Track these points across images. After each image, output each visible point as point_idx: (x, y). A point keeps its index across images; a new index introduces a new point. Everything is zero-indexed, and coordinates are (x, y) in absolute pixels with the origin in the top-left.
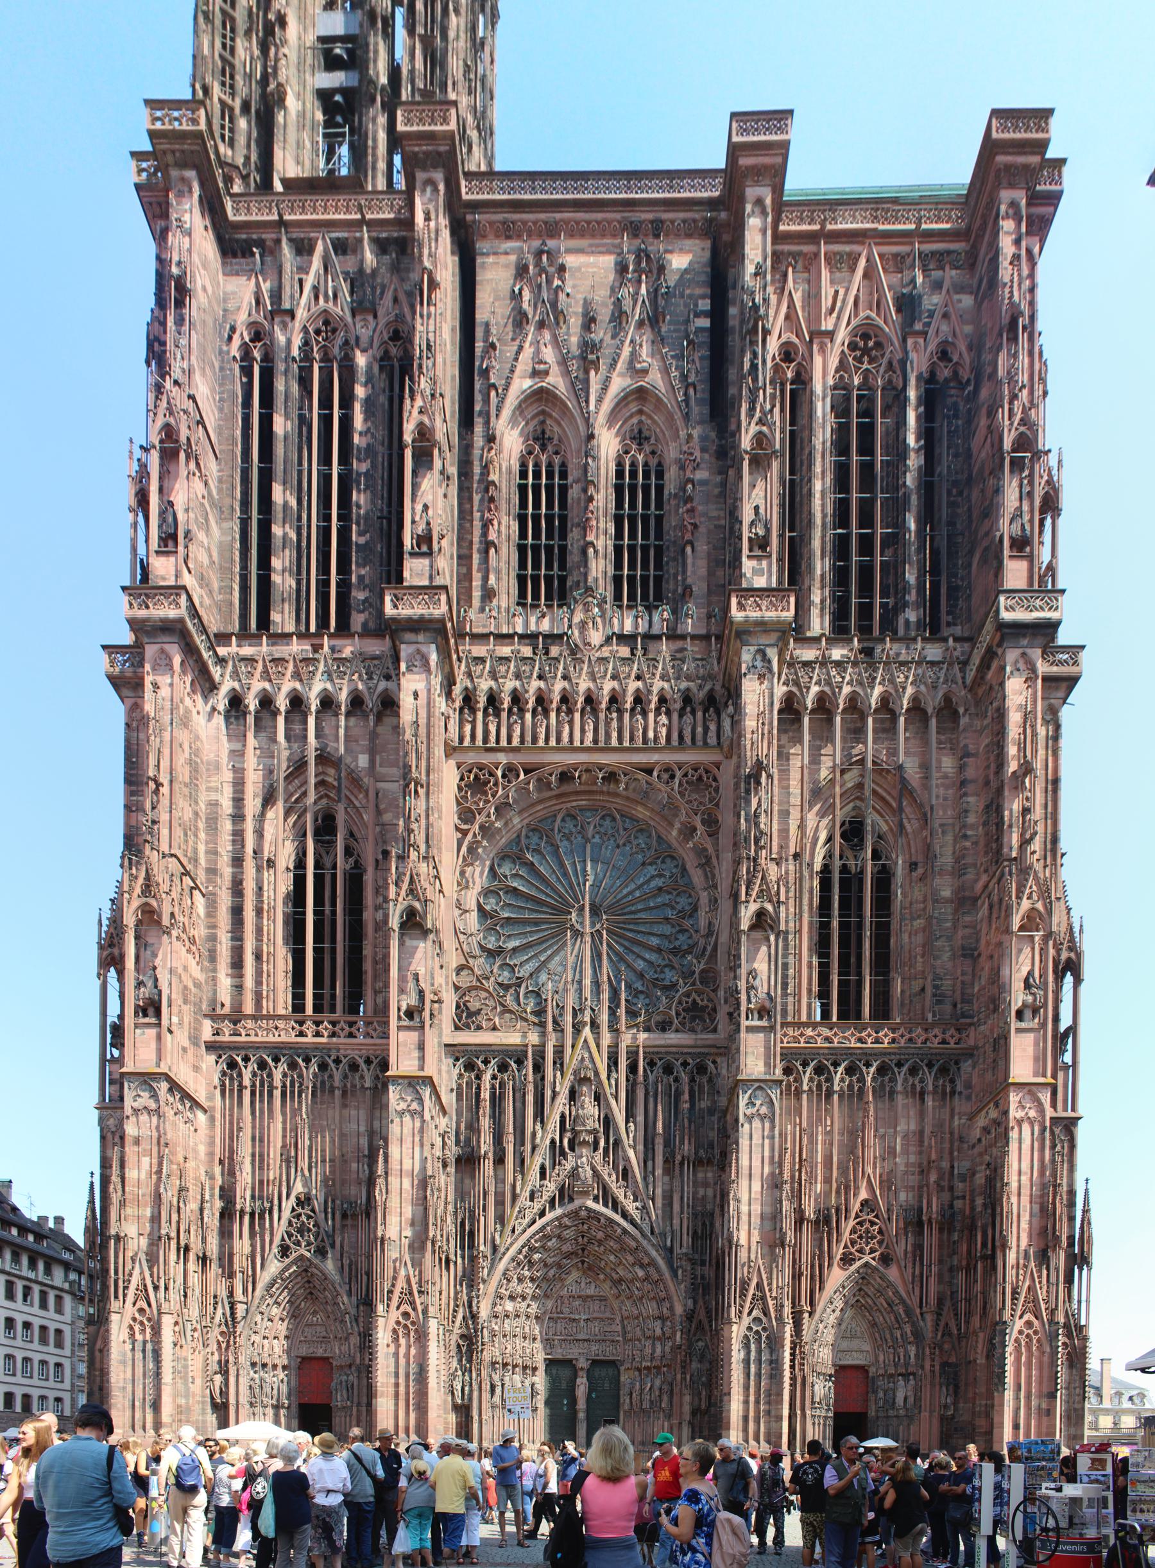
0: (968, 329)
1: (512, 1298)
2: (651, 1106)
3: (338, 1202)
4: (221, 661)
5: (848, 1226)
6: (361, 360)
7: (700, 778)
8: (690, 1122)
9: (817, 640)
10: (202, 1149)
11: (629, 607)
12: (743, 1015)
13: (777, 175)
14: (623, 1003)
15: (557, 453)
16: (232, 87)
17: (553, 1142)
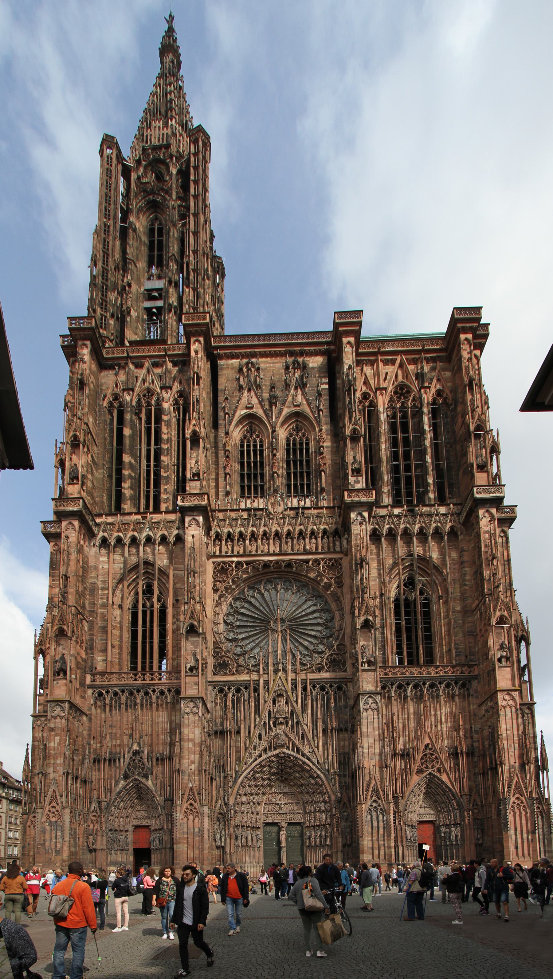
0: (449, 384)
1: (245, 795)
2: (315, 705)
3: (154, 754)
4: (98, 525)
5: (418, 757)
6: (165, 405)
7: (333, 565)
8: (335, 711)
9: (386, 507)
10: (85, 733)
11: (295, 497)
12: (360, 665)
13: (357, 334)
14: (299, 660)
15: (258, 436)
16: (106, 309)
17: (265, 723)
